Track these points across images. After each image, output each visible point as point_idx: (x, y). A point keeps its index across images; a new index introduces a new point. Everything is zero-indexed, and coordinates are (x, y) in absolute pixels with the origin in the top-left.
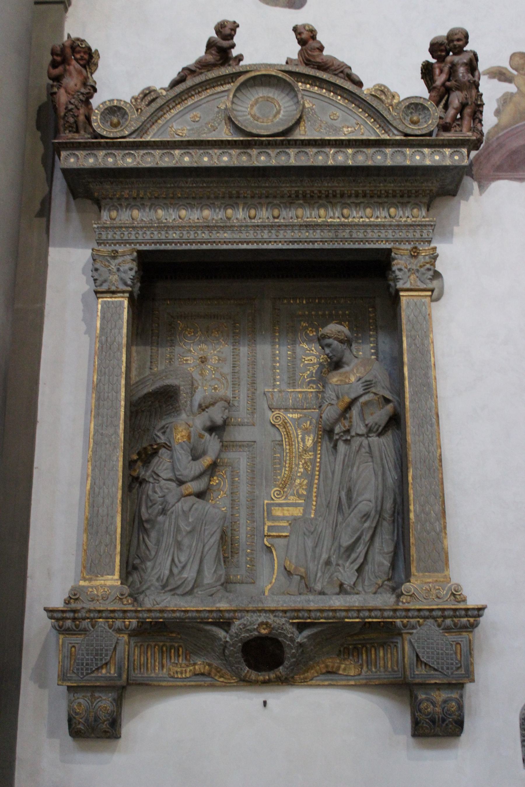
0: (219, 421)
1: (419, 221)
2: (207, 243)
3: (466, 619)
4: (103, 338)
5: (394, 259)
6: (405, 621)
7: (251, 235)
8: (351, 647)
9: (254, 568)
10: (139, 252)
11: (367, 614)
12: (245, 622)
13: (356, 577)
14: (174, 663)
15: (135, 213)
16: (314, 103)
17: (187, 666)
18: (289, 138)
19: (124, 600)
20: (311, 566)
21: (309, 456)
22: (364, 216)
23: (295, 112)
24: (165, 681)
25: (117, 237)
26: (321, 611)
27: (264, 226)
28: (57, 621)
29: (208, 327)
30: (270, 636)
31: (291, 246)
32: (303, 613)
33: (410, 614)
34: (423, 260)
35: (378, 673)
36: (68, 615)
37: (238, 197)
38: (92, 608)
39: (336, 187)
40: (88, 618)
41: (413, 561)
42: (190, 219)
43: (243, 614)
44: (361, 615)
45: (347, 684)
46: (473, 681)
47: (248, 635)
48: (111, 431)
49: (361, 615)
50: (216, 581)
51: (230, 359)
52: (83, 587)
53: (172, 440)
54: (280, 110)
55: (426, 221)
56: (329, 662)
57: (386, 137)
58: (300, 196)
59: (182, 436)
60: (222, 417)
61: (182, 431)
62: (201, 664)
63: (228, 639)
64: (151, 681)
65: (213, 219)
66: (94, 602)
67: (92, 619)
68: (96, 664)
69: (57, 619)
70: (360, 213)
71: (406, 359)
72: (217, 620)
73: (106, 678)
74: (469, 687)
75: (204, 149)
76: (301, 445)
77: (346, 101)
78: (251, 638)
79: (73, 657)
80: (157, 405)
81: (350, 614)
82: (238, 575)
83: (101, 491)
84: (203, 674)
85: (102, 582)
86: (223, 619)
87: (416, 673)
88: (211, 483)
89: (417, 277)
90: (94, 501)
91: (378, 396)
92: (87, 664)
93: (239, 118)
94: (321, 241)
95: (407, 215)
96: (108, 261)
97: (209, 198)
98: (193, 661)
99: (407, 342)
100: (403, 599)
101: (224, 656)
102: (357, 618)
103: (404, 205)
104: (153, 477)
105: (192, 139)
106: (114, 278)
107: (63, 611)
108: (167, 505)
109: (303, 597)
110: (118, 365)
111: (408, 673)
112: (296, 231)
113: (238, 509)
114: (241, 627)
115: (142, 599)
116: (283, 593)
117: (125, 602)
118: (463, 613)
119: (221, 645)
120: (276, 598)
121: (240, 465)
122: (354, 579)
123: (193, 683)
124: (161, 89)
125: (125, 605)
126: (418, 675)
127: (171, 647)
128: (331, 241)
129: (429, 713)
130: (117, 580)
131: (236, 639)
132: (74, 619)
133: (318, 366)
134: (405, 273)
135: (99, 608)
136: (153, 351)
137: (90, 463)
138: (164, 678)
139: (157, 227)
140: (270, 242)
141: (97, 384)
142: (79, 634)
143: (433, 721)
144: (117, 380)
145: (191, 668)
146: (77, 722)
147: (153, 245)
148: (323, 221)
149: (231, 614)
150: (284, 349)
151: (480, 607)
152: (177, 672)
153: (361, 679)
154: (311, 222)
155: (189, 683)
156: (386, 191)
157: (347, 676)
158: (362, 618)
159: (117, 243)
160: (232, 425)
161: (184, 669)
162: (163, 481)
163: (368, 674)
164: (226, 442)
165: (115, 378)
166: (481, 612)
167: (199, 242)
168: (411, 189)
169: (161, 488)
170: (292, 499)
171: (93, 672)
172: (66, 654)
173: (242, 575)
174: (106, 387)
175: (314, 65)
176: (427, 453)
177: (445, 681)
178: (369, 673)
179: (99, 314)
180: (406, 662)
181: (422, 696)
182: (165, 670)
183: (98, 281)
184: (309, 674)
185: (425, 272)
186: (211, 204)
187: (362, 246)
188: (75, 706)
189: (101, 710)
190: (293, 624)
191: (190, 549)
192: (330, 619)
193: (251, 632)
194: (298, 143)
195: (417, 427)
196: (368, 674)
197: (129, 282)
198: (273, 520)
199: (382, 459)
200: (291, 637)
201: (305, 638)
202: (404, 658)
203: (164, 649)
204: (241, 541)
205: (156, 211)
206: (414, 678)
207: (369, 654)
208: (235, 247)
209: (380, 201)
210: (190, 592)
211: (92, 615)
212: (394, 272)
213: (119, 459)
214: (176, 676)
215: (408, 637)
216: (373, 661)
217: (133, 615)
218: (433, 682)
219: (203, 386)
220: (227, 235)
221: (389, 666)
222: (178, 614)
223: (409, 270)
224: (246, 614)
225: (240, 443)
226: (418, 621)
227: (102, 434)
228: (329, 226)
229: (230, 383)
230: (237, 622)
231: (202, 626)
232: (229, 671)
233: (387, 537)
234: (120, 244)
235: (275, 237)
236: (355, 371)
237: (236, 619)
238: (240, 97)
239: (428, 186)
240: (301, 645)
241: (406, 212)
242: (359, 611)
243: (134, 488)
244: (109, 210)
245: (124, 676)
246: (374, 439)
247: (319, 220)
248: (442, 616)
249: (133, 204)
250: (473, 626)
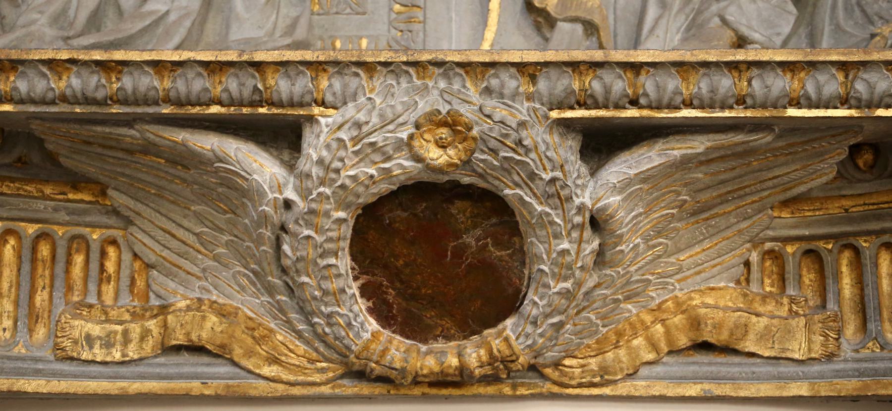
8: (790, 249)
9: (419, 14)
12: (362, 117)
13: (792, 19)
17: (135, 316)
24: (38, 373)
43: (354, 83)
45: (777, 393)
47: (372, 171)
62: (188, 308)
63: (290, 194)
72: (245, 110)
78: (384, 188)
82: (361, 38)
86: (271, 104)
98: (159, 296)
101: (284, 271)
114: (343, 135)
131: (322, 189)
138: (36, 360)
145: (152, 324)
149: (302, 84)
152: (89, 340)
161: (119, 328)
163: (865, 353)
182: (41, 332)
184: (622, 352)
192: (723, 108)
193: (389, 159)
196: (865, 353)
200: (553, 180)
214: (85, 356)
222: (74, 82)
230: (327, 119)
231: (180, 136)
232: (299, 335)
237: (323, 104)
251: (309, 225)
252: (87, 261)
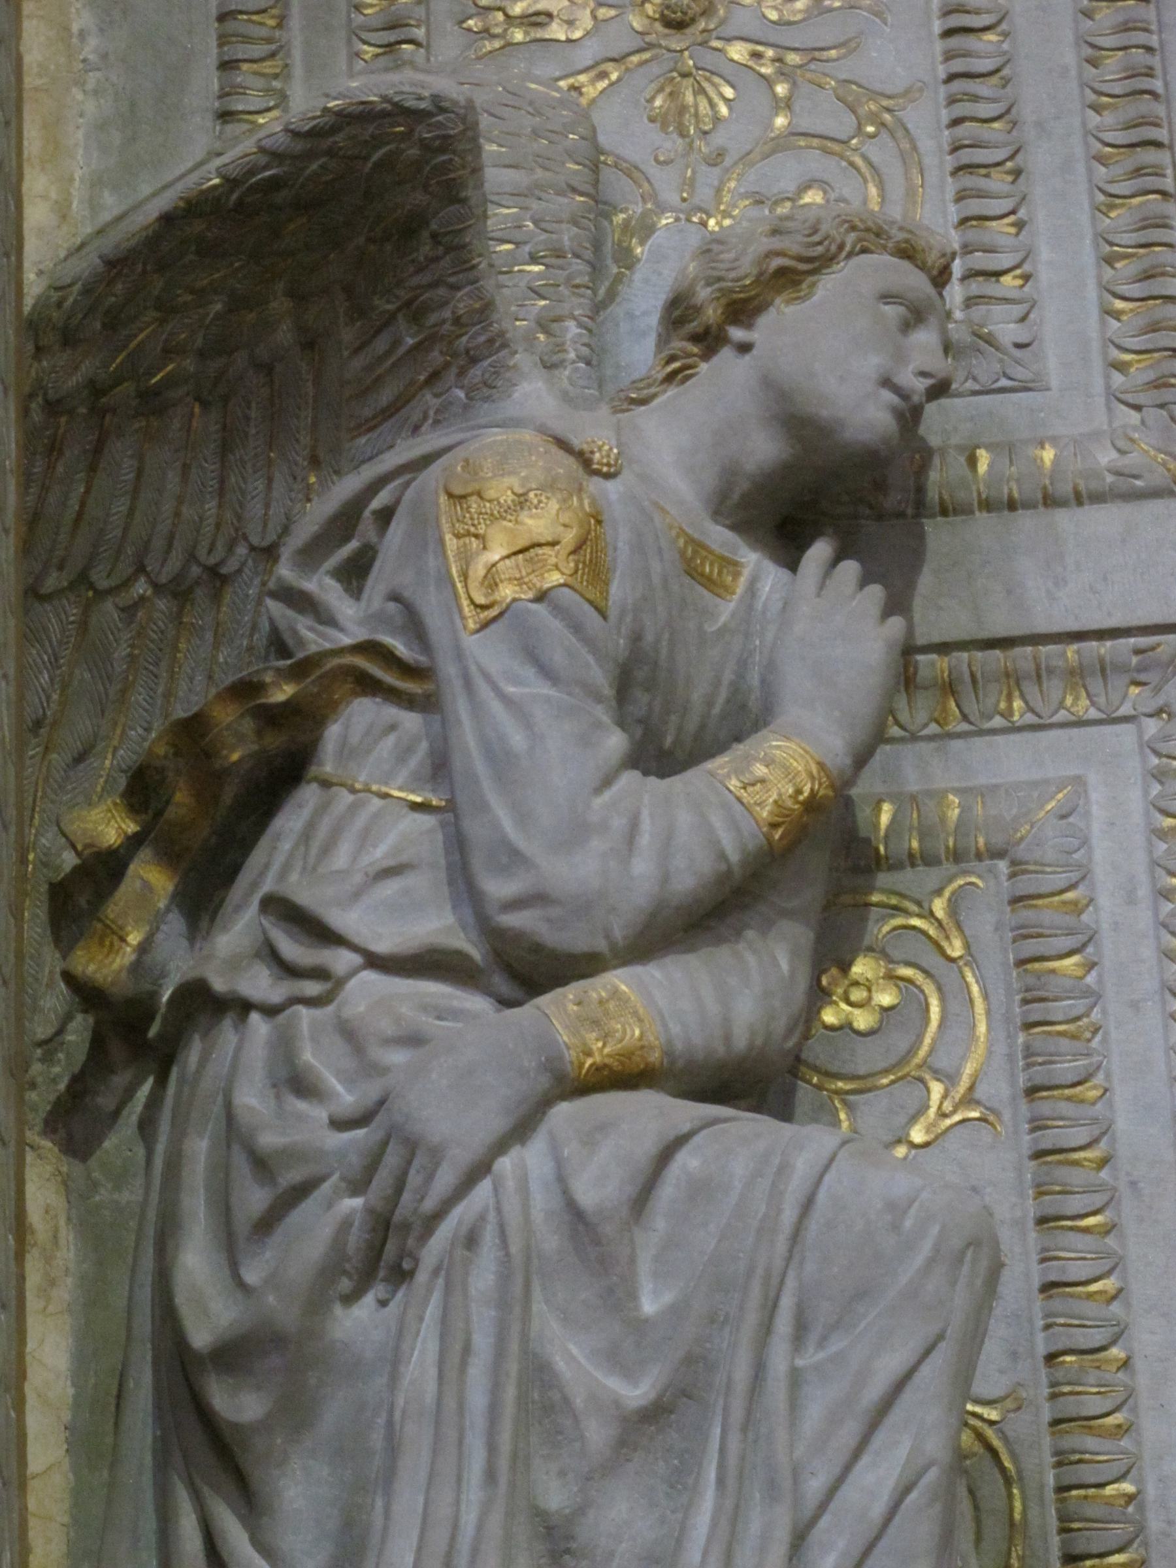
53: (434, 621)
60: (887, 382)
61: (522, 501)
80: (284, 335)
88: (829, 1017)
104: (272, 955)
108: (414, 1179)
113: (1108, 1230)
121: (1085, 842)
160: (987, 505)
162: (369, 976)
164: (943, 648)
169: (349, 1033)
204: (1155, 1524)
219: (690, 210)
225: (1071, 651)
229: (929, 161)
243: (116, 1114)
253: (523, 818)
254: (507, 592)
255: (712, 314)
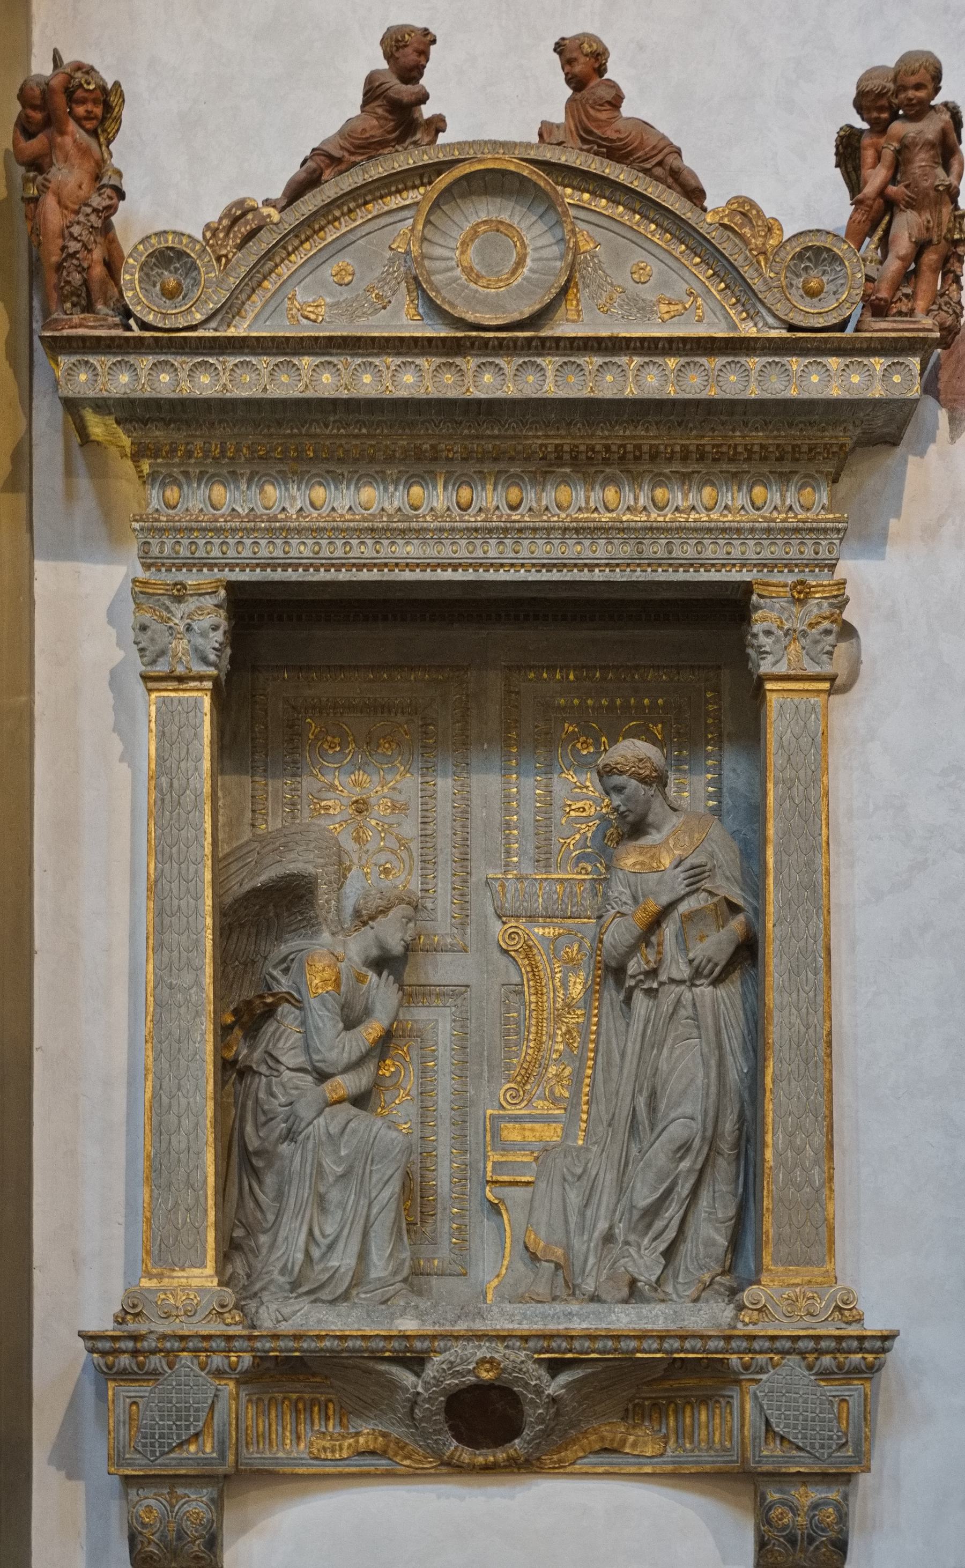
0: (396, 946)
1: (814, 521)
2: (370, 567)
3: (860, 1356)
4: (164, 780)
5: (758, 608)
6: (747, 1358)
7: (461, 550)
10: (231, 587)
11: (677, 1344)
12: (452, 1359)
14: (319, 1432)
15: (218, 492)
16: (599, 240)
18: (543, 334)
19: (226, 1315)
20: (578, 1244)
21: (574, 1019)
22: (699, 507)
23: (558, 264)
25: (183, 552)
26: (592, 1338)
27: (490, 531)
28: (103, 1357)
29: (370, 732)
30: (497, 1383)
31: (545, 576)
32: (559, 1341)
33: (756, 1345)
34: (815, 611)
35: (697, 1453)
36: (122, 1345)
37: (435, 459)
38: (170, 1332)
39: (643, 437)
40: (161, 1351)
41: (767, 1243)
42: (333, 509)
43: (449, 1344)
44: (666, 1345)
46: (868, 1469)
48: (187, 978)
49: (666, 1345)
50: (395, 1273)
51: (416, 803)
52: (148, 1290)
54: (525, 255)
55: (827, 520)
56: (606, 1431)
57: (749, 330)
58: (566, 457)
59: (324, 981)
63: (420, 1389)
64: (277, 1464)
65: (383, 510)
66: (171, 1319)
67: (168, 1352)
68: (179, 1436)
69: (104, 1353)
70: (691, 495)
71: (771, 831)
73: (197, 1461)
74: (864, 1481)
75: (362, 355)
76: (561, 993)
77: (668, 236)
79: (134, 1423)
81: (645, 1345)
83: (174, 1101)
84: (372, 1453)
85: (184, 1280)
87: (765, 1453)
89: (803, 648)
90: (160, 1123)
91: (716, 899)
92: (162, 1436)
93: (436, 278)
94: (607, 565)
95: (788, 502)
96: (167, 609)
97: (372, 459)
99: (776, 792)
100: (746, 1316)
102: (658, 1351)
103: (785, 478)
105: (339, 334)
106: (181, 645)
107: (114, 1339)
109: (558, 1307)
110: (196, 838)
111: (749, 1454)
112: (556, 542)
114: (444, 1366)
115: (253, 1310)
116: (521, 1299)
117: (229, 1321)
118: (855, 1344)
119: (408, 1400)
120: (508, 1307)
122: (659, 1272)
123: (354, 1469)
124: (267, 202)
125: (227, 1325)
126: (766, 1456)
127: (313, 1402)
128: (628, 565)
129: (786, 1527)
130: (211, 1276)
132: (135, 1353)
133: (597, 822)
134: (777, 641)
135: (181, 1333)
136: (257, 786)
137: (149, 1045)
139: (266, 529)
140: (502, 565)
141: (156, 882)
142: (144, 1380)
143: (792, 1540)
144: (196, 872)
146: (145, 1541)
147: (258, 570)
148: (613, 520)
149: (427, 1344)
150: (528, 782)
151: (885, 1333)
153: (665, 1463)
154: (586, 520)
155: (347, 1470)
156: (746, 449)
157: (638, 1456)
158: (666, 1352)
159: (184, 565)
165: (192, 868)
166: (887, 1344)
167: (354, 565)
168: (799, 442)
170: (541, 1106)
171: (172, 1450)
172: (122, 1419)
173: (442, 1260)
174: (175, 886)
175: (600, 146)
176: (803, 1029)
177: (816, 1470)
178: (680, 1452)
179: (153, 725)
180: (746, 1433)
181: (773, 1496)
182: (302, 1445)
183: (147, 653)
185: (818, 637)
186: (377, 472)
187: (691, 576)
188: (141, 1513)
189: (188, 1519)
190: (539, 1361)
191: (344, 1209)
194: (562, 344)
195: (786, 976)
197: (212, 657)
198: (503, 1149)
199: (718, 1034)
201: (563, 1387)
202: (743, 1426)
203: (301, 1406)
205: (262, 490)
206: (759, 1462)
207: (680, 1419)
208: (428, 576)
209: (733, 468)
210: (345, 1296)
211: (168, 1345)
212: (755, 636)
213: (207, 1037)
215: (753, 1387)
216: (688, 1429)
217: (246, 1344)
218: (794, 1470)
220: (411, 550)
221: (717, 1439)
222: (327, 1344)
223: (786, 634)
224: (455, 1344)
226: (771, 1359)
227: (171, 987)
228: (623, 530)
231: (371, 1364)
233: (724, 1188)
234: (190, 567)
235: (512, 555)
236: (671, 843)
238: (437, 223)
239: (836, 437)
240: (554, 1400)
241: (788, 494)
242: (662, 1338)
244: (163, 485)
245: (231, 1458)
246: (705, 991)
247: (606, 517)
248: (816, 1350)
249: (212, 471)
250: (873, 1369)
251: (428, 1402)
252: (320, 1411)
253: (321, 1043)
254: (320, 991)
255: (365, 918)
